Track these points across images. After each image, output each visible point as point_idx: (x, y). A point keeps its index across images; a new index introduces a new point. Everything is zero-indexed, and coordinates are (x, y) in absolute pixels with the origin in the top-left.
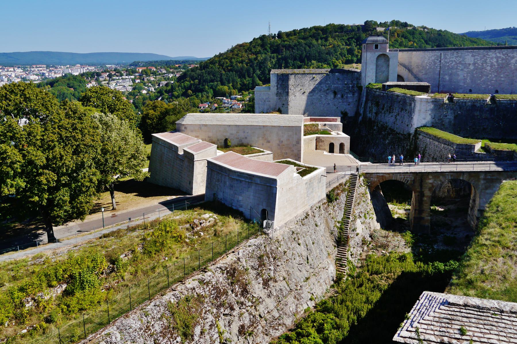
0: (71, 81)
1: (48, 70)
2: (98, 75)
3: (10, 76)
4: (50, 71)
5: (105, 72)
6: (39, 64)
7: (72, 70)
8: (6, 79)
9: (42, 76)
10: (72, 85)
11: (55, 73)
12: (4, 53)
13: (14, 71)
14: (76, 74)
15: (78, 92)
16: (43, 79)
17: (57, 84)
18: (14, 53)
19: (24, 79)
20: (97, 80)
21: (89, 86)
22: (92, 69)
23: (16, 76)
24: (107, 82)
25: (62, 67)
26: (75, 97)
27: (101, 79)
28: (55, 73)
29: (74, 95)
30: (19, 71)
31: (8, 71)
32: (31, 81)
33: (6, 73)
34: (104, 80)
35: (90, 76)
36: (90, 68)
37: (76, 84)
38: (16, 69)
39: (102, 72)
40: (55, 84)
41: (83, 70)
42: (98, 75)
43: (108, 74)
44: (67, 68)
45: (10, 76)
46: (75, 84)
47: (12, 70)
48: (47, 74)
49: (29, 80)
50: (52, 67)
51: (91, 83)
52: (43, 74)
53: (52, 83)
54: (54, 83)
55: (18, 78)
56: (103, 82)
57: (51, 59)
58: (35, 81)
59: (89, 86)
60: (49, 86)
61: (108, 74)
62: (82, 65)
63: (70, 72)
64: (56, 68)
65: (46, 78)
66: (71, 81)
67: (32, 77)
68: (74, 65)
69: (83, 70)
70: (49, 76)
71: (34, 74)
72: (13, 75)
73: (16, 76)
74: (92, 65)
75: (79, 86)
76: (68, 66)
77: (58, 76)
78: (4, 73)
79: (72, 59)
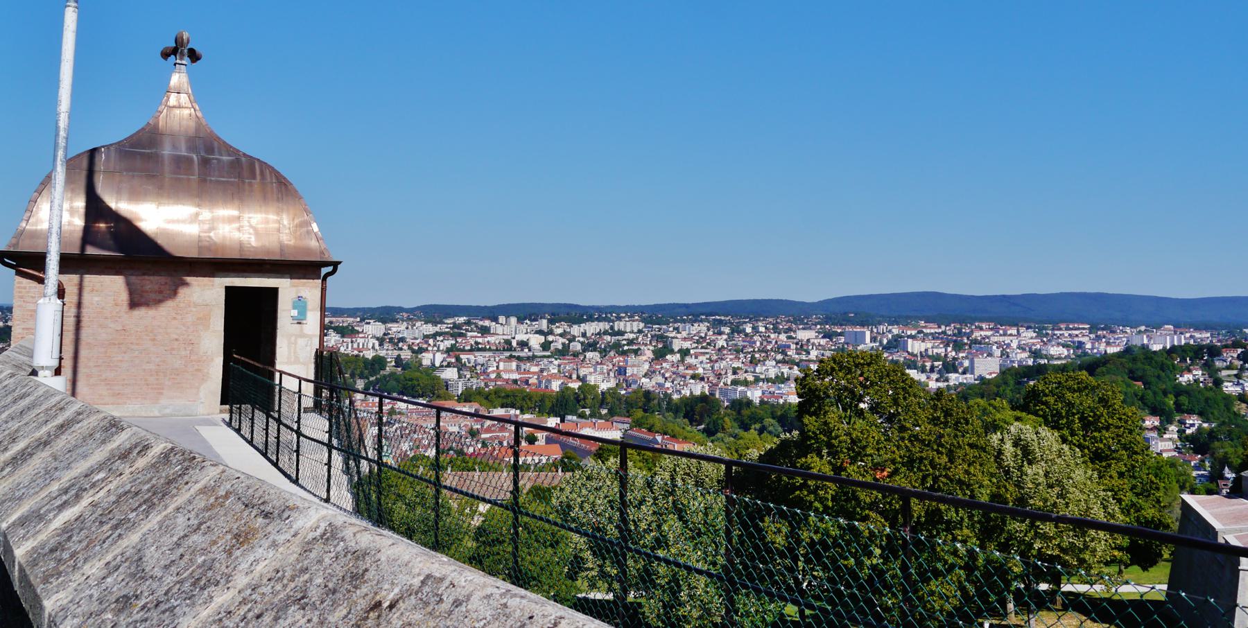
0: (1139, 365)
1: (1092, 336)
2: (1214, 352)
3: (1008, 345)
4: (1098, 338)
5: (1235, 345)
6: (1073, 322)
7: (1149, 338)
8: (998, 352)
9: (1078, 348)
10: (1139, 373)
11: (1108, 344)
12: (1004, 296)
13: (1019, 334)
14: (1156, 347)
15: (1155, 393)
16: (1079, 356)
17: (1104, 369)
18: (1024, 296)
19: (1036, 354)
20: (1208, 367)
21: (1185, 379)
22: (1205, 337)
23: (1019, 347)
24: (1235, 372)
25: (1128, 330)
26: (1145, 404)
27: (1218, 364)
28: (1108, 344)
29: (1142, 399)
30: (1028, 336)
31: (1005, 334)
32: (1051, 357)
33: (1001, 339)
34: (1228, 368)
35: (1191, 354)
36: (1197, 335)
37: (1150, 371)
38: (1022, 330)
39: (1226, 347)
40: (1099, 370)
41: (1180, 340)
42: (1214, 352)
43: (1240, 351)
44: (1140, 332)
45: (1008, 345)
46: (1148, 373)
47: (1014, 331)
48: (1089, 346)
49: (1046, 357)
50: (1103, 329)
51: (1190, 371)
52: (1081, 345)
53: (1094, 365)
54: (1098, 366)
55: (1024, 350)
56: (1224, 373)
57: (1102, 310)
58: (1059, 358)
59: (1185, 379)
60: (1085, 372)
61: (1240, 351)
62: (1179, 327)
63: (1145, 341)
64: (1113, 332)
65: (1085, 354)
66: (1139, 365)
67: (1055, 350)
68: (1158, 327)
69: (1180, 340)
70: (1092, 349)
71: (1059, 344)
72: (1014, 345)
73: (1019, 347)
74: (1206, 329)
75: (1159, 377)
76: (1143, 328)
77: (1111, 350)
78: (996, 339)
79: (1154, 311)
